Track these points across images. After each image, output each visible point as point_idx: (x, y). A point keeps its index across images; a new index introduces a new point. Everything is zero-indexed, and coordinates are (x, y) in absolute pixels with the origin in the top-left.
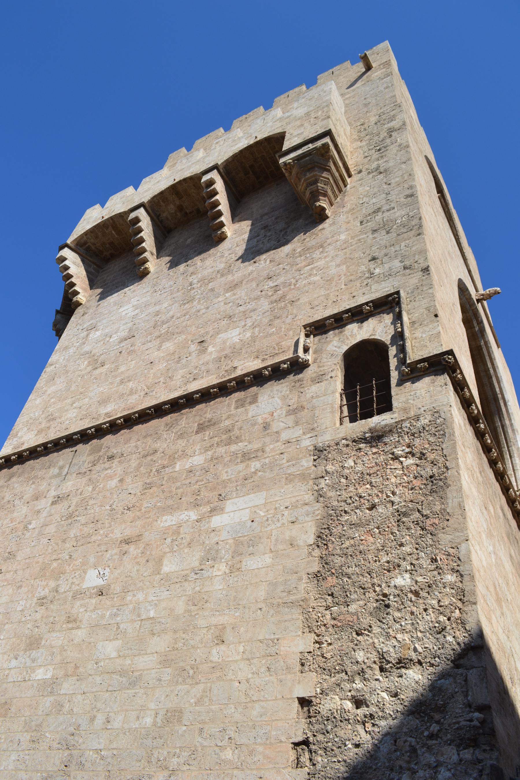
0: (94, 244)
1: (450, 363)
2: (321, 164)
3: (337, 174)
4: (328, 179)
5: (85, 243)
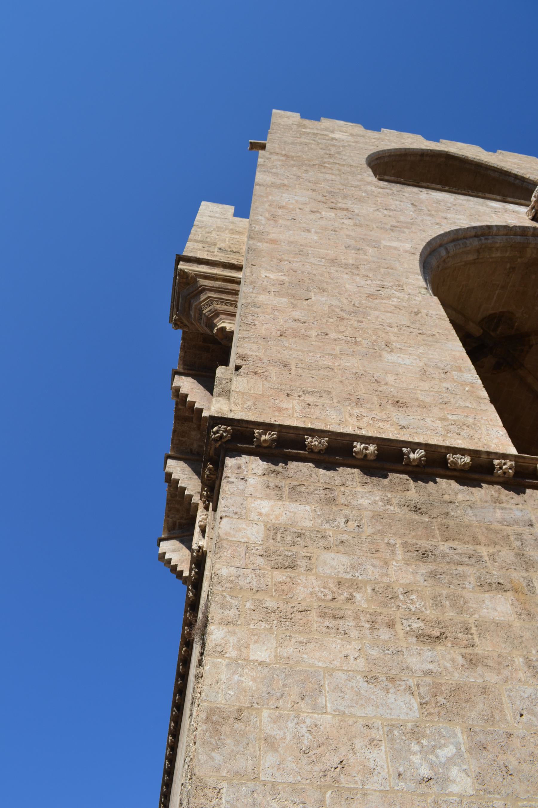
0: (181, 518)
1: (221, 437)
2: (193, 292)
3: (218, 284)
4: (209, 297)
5: (174, 524)
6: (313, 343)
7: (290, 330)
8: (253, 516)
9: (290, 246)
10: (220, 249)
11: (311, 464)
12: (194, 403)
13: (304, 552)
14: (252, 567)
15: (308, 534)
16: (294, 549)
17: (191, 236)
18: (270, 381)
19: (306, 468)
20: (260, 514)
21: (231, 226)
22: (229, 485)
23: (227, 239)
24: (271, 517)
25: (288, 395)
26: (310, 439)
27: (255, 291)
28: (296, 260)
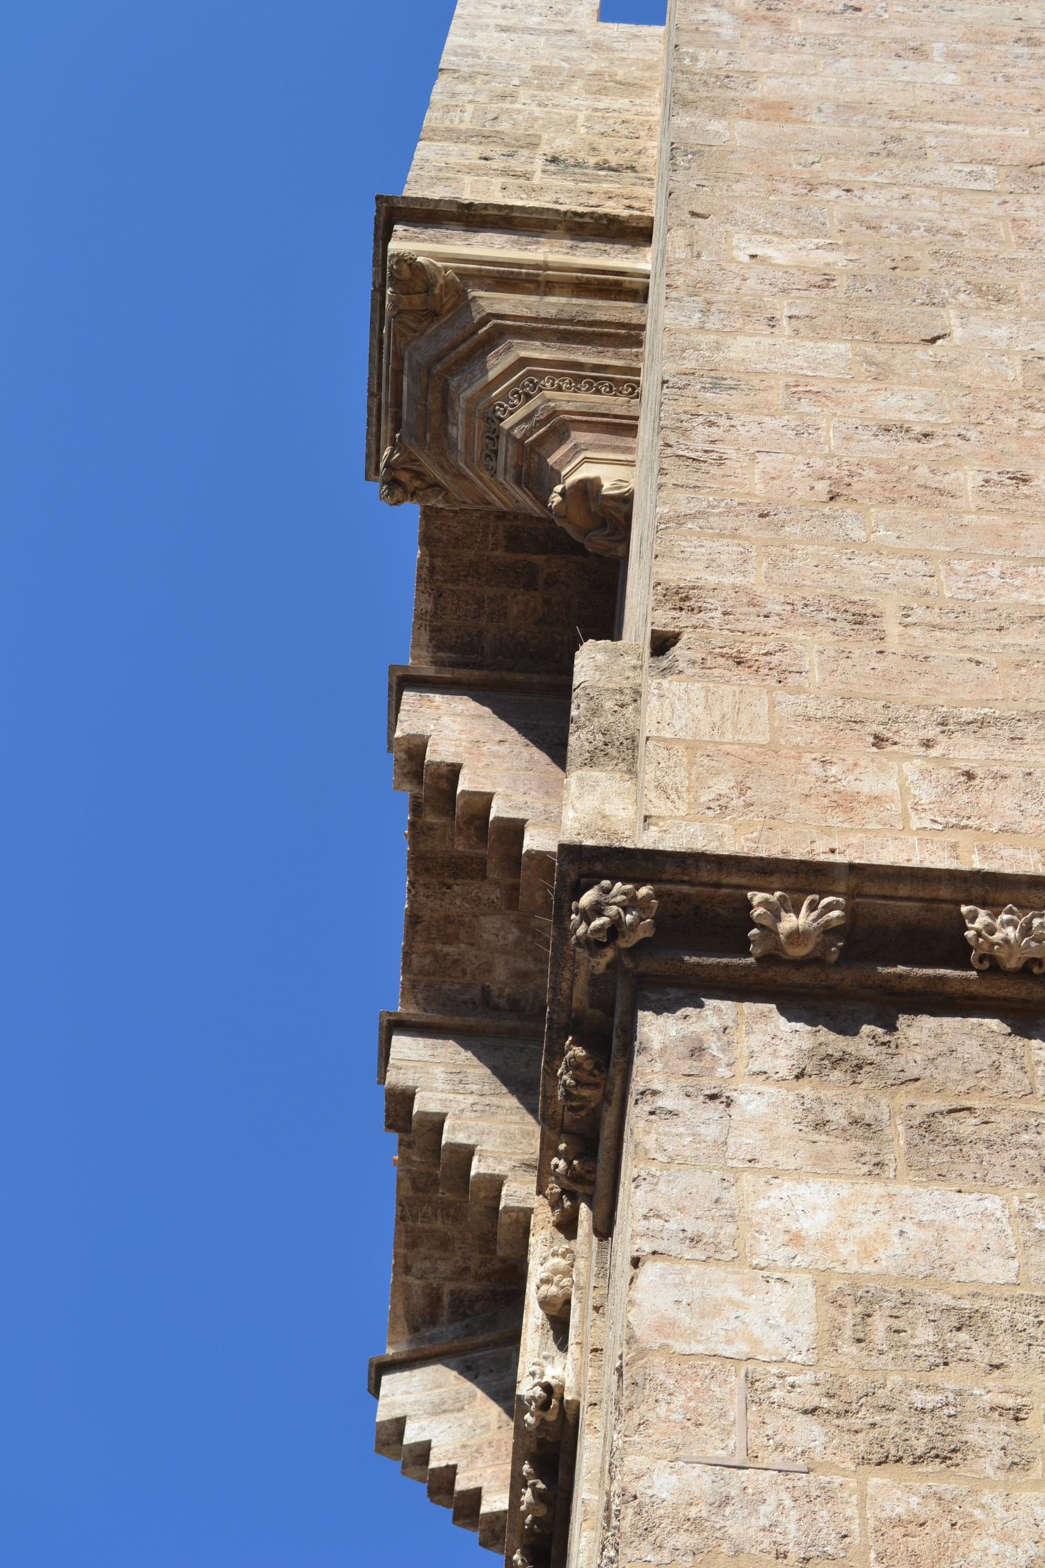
0: (462, 1273)
1: (615, 929)
2: (454, 347)
3: (553, 305)
4: (523, 362)
5: (434, 1298)
6: (967, 519)
7: (869, 474)
8: (768, 1249)
9: (845, 123)
10: (554, 160)
11: (994, 1024)
12: (489, 797)
13: (990, 1392)
14: (776, 1459)
15: (1001, 1315)
16: (950, 1379)
17: (432, 118)
18: (800, 690)
19: (976, 1037)
20: (796, 1239)
21: (594, 63)
22: (660, 1125)
23: (581, 117)
24: (844, 1250)
25: (879, 741)
26: (983, 918)
27: (714, 322)
28: (873, 178)
